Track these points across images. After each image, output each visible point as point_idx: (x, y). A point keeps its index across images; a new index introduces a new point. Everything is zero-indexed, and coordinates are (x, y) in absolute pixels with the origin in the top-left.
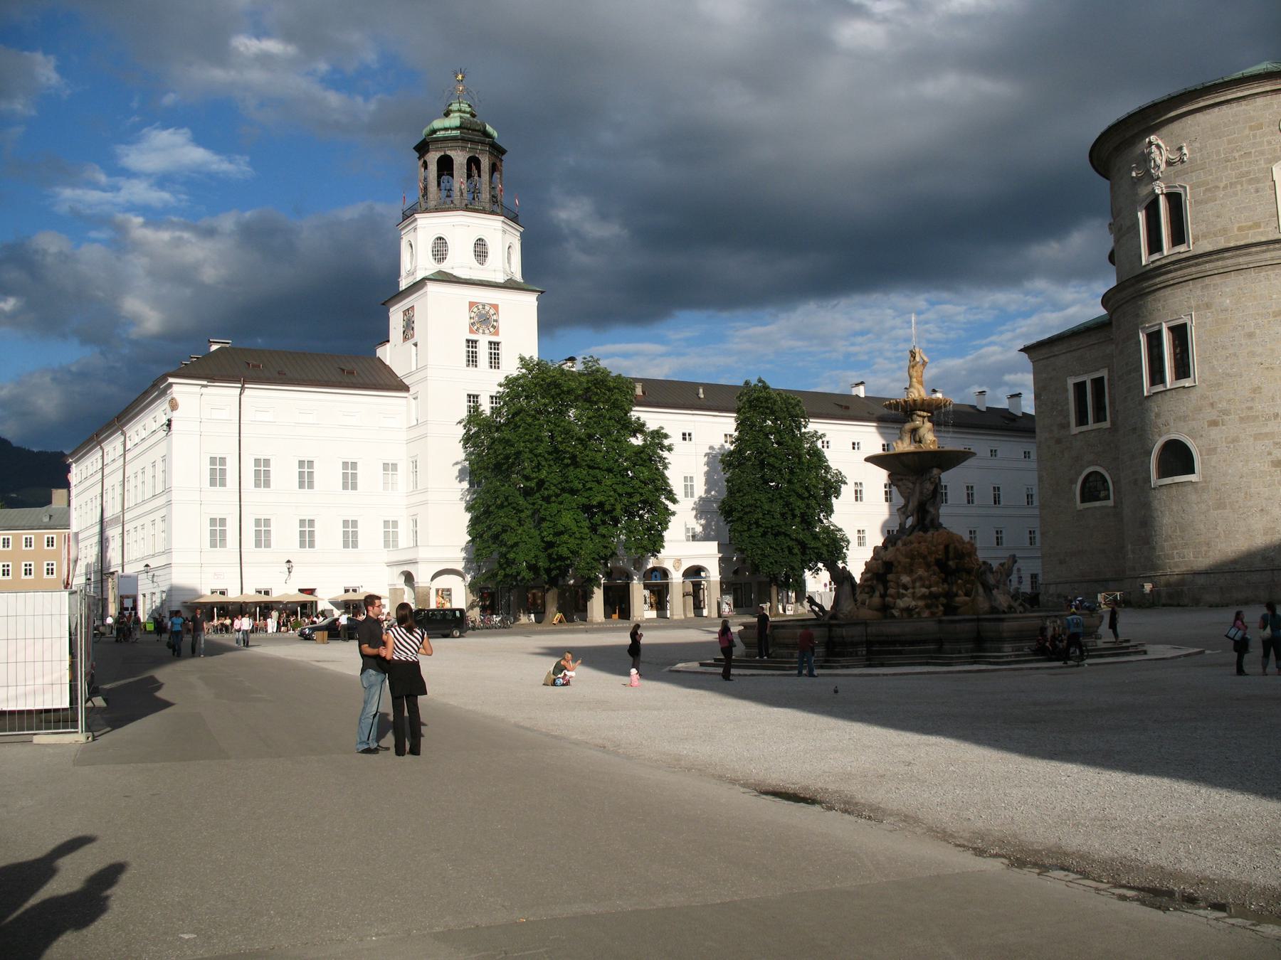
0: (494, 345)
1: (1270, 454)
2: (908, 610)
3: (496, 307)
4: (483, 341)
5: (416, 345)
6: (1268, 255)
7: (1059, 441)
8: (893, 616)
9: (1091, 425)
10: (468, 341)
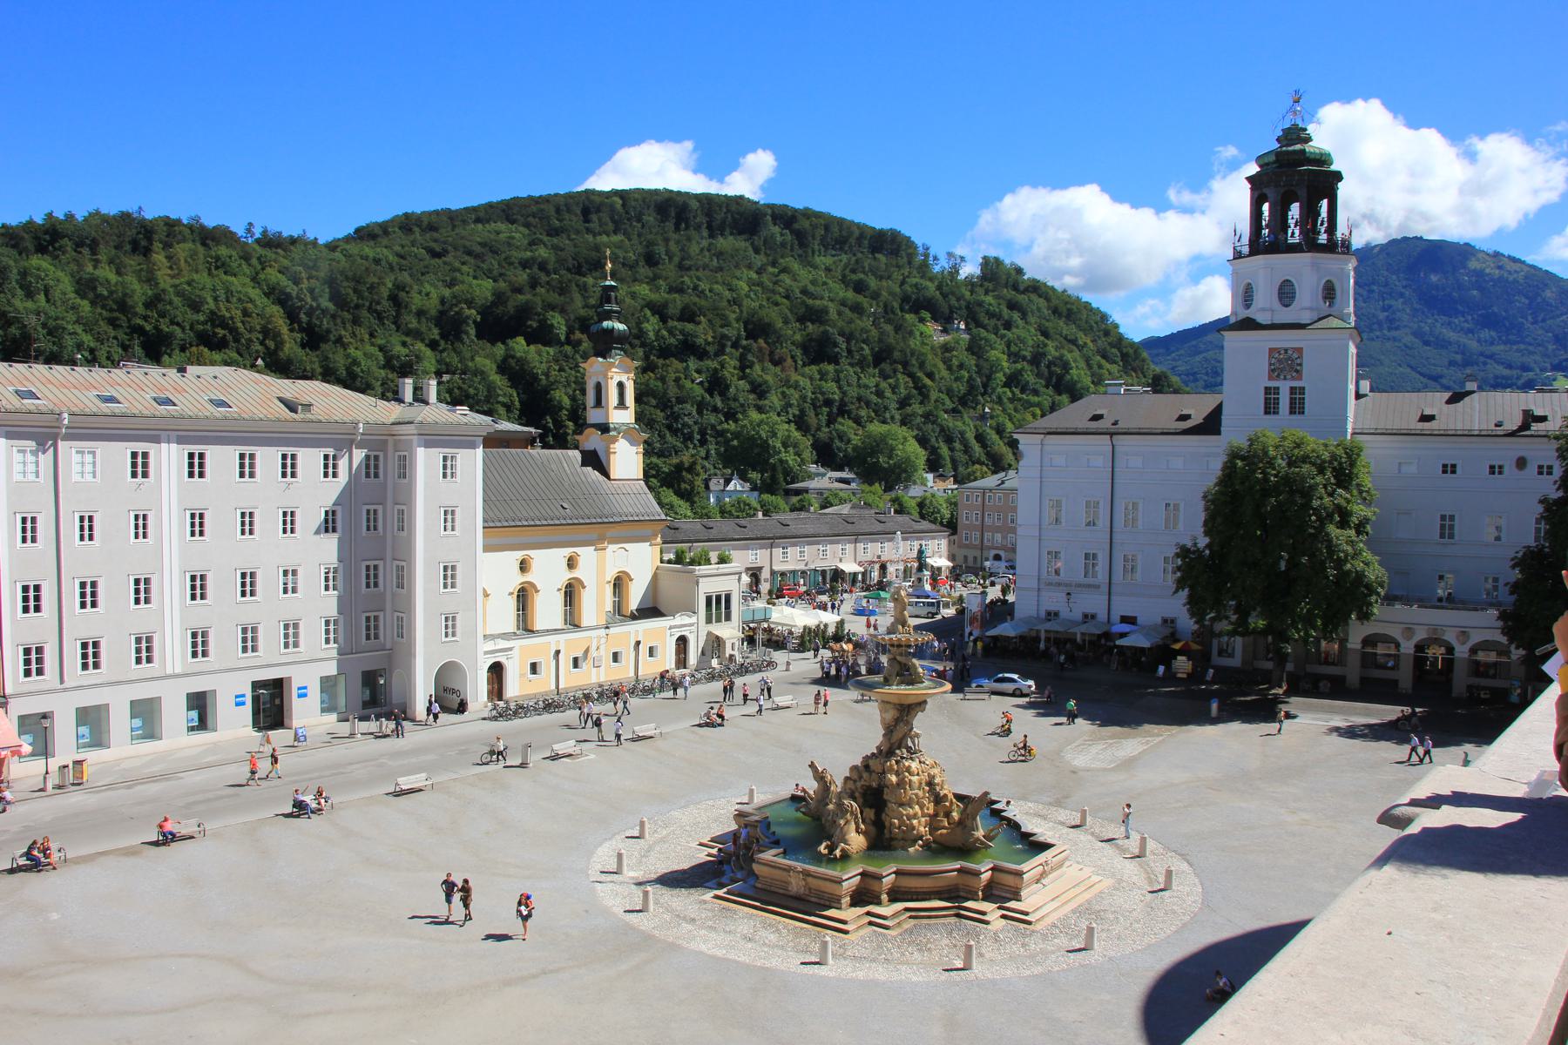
3: (1300, 350)
4: (1284, 387)
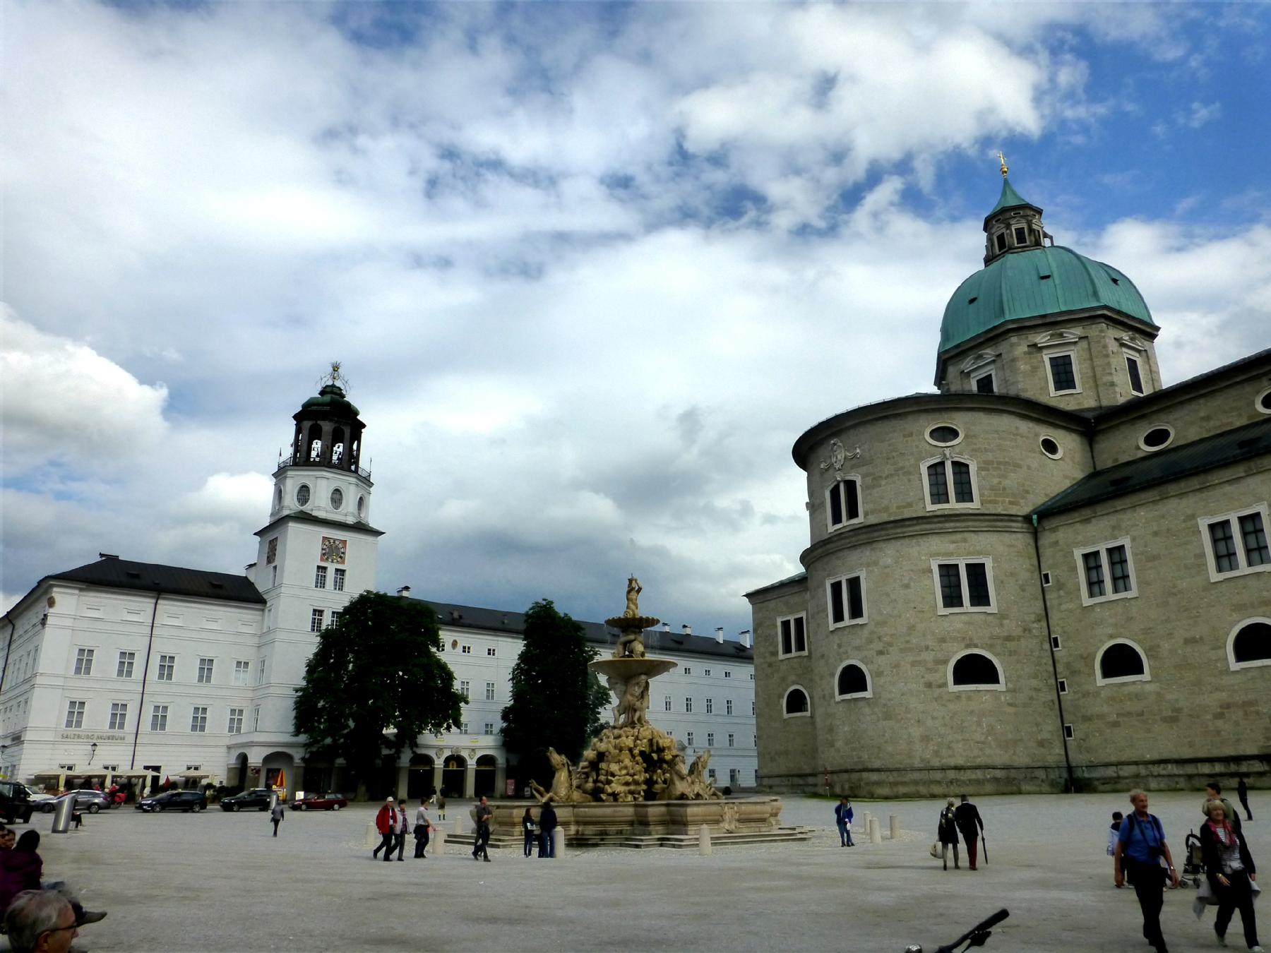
0: (341, 572)
2: (615, 796)
4: (331, 568)
5: (275, 568)
6: (917, 528)
7: (770, 665)
8: (602, 800)
9: (794, 653)
10: (319, 567)
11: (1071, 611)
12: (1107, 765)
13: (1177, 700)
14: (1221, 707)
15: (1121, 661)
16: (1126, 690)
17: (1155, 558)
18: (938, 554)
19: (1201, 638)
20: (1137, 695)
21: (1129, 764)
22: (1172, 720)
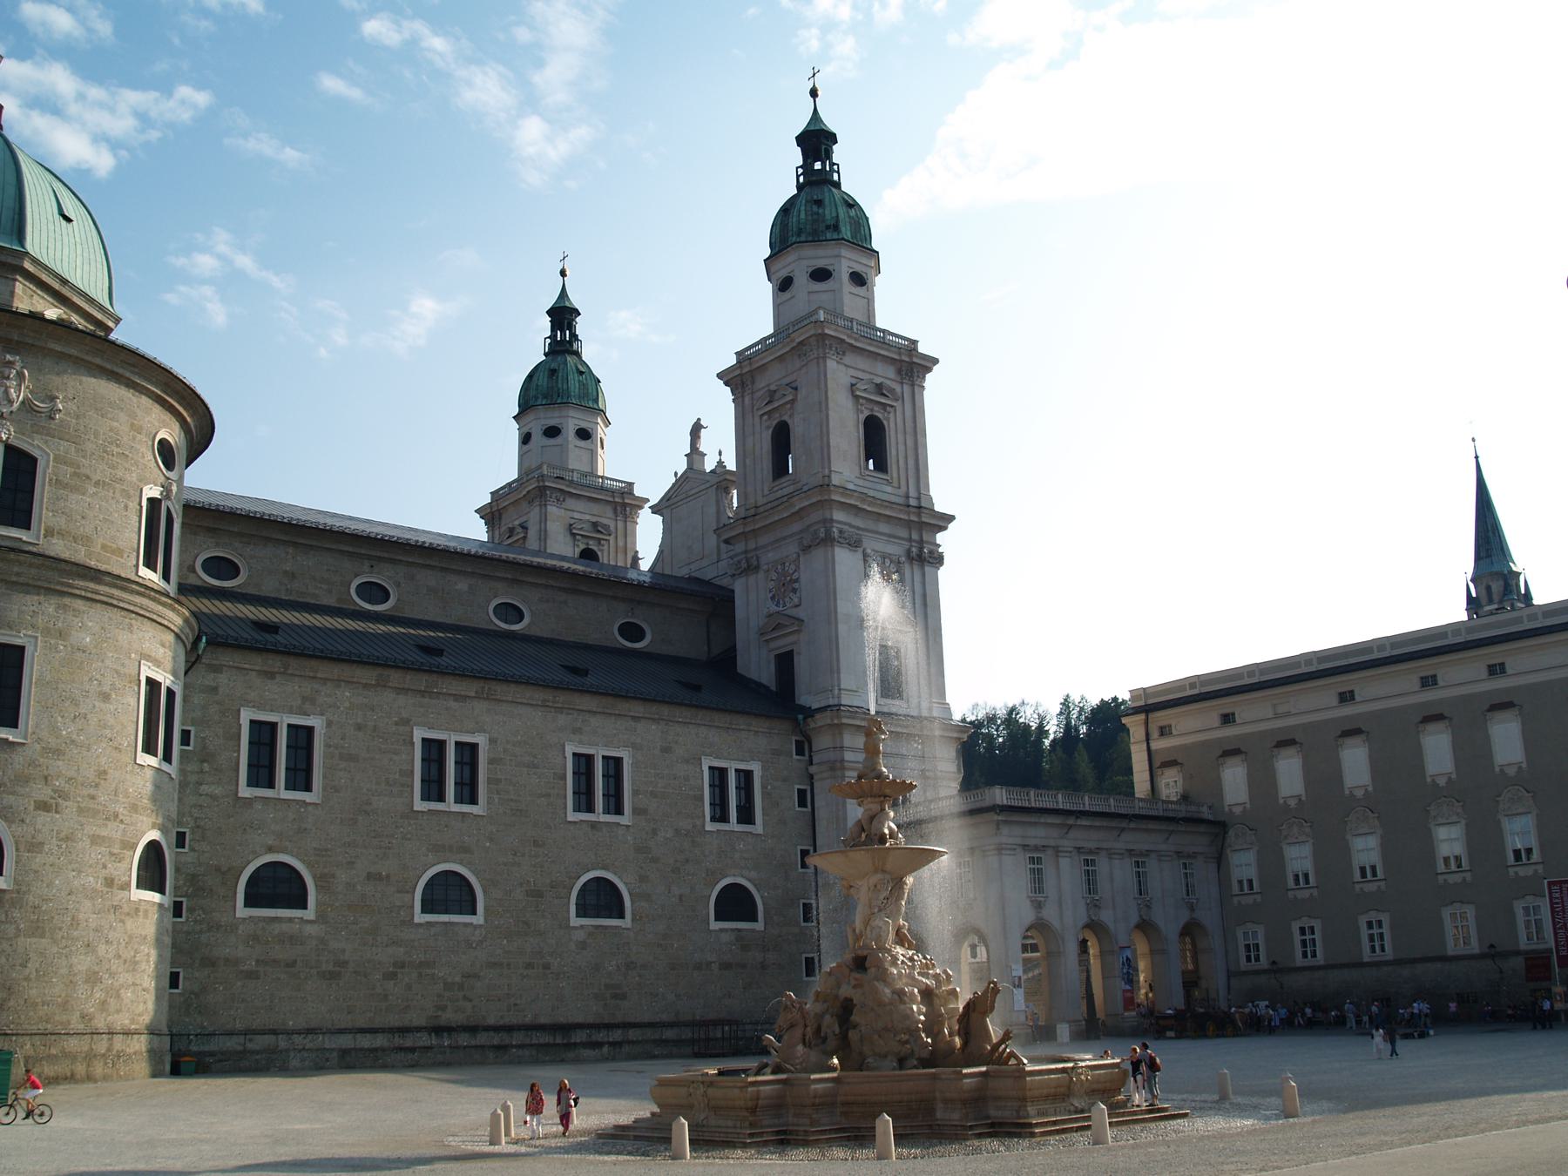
1: (105, 867)
11: (213, 797)
12: (231, 1034)
13: (344, 951)
14: (395, 964)
15: (276, 887)
16: (277, 928)
17: (352, 758)
18: (148, 658)
19: (388, 876)
20: (291, 937)
21: (263, 1032)
22: (332, 976)
